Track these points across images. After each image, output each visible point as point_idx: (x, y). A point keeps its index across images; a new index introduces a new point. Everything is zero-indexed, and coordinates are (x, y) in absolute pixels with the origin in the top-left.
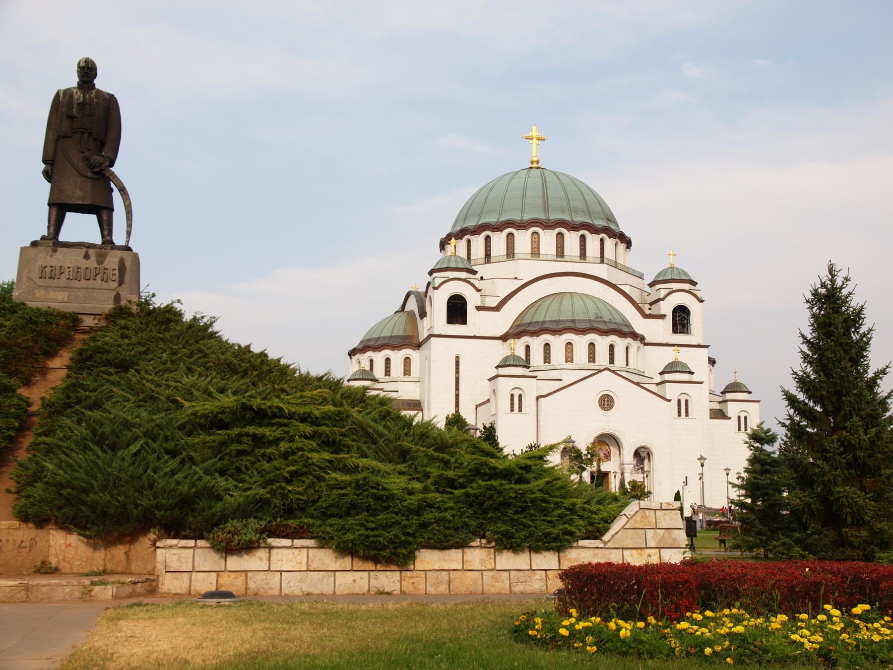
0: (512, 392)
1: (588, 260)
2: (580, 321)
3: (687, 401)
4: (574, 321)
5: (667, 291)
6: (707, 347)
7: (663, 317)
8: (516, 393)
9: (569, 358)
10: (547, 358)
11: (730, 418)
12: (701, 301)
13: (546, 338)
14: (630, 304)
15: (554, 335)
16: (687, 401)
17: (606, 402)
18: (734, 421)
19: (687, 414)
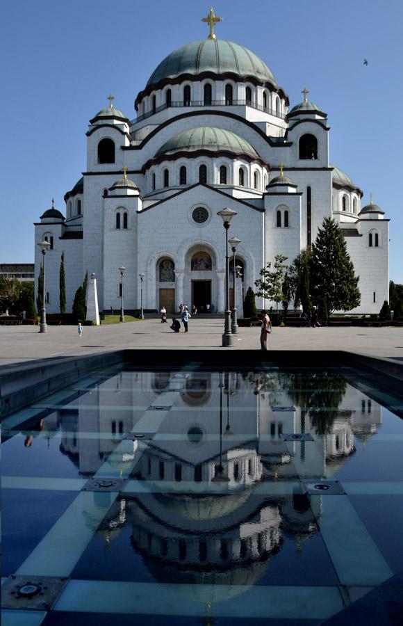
0: (118, 211)
1: (234, 103)
2: (194, 146)
3: (286, 213)
4: (188, 147)
5: (295, 122)
6: (332, 169)
7: (289, 144)
8: (122, 212)
9: (183, 179)
10: (166, 184)
11: (361, 235)
12: (328, 129)
13: (165, 164)
14: (259, 135)
15: (170, 160)
16: (286, 213)
17: (200, 215)
18: (365, 239)
19: (287, 224)
